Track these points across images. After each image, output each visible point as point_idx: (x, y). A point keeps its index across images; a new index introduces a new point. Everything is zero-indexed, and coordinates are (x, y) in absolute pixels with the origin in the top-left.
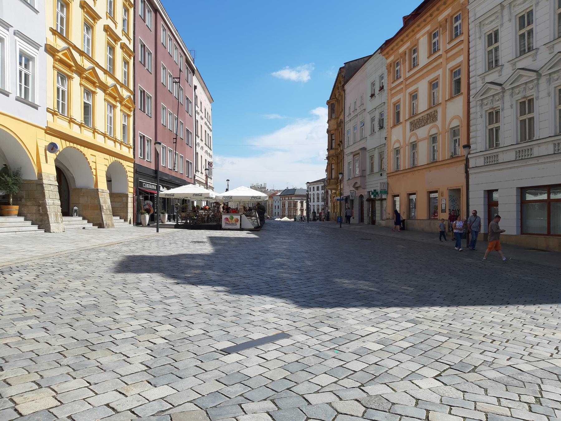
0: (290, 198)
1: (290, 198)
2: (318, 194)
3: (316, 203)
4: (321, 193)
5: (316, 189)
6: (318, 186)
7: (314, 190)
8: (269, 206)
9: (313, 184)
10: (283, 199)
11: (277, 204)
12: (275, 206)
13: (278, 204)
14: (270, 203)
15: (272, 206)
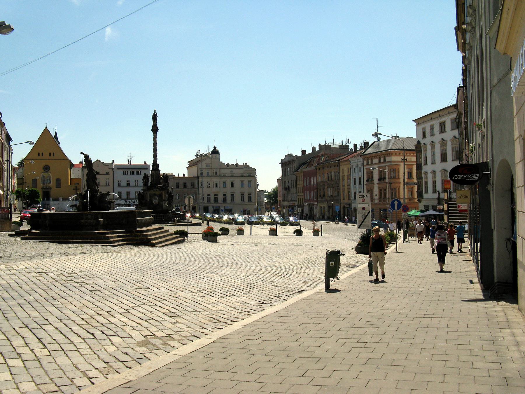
0: (382, 160)
1: (382, 160)
2: (443, 142)
3: (439, 166)
4: (451, 137)
5: (437, 129)
6: (442, 120)
7: (432, 135)
8: (343, 179)
9: (429, 118)
10: (368, 163)
11: (355, 175)
12: (355, 179)
13: (360, 174)
14: (346, 173)
15: (348, 179)
